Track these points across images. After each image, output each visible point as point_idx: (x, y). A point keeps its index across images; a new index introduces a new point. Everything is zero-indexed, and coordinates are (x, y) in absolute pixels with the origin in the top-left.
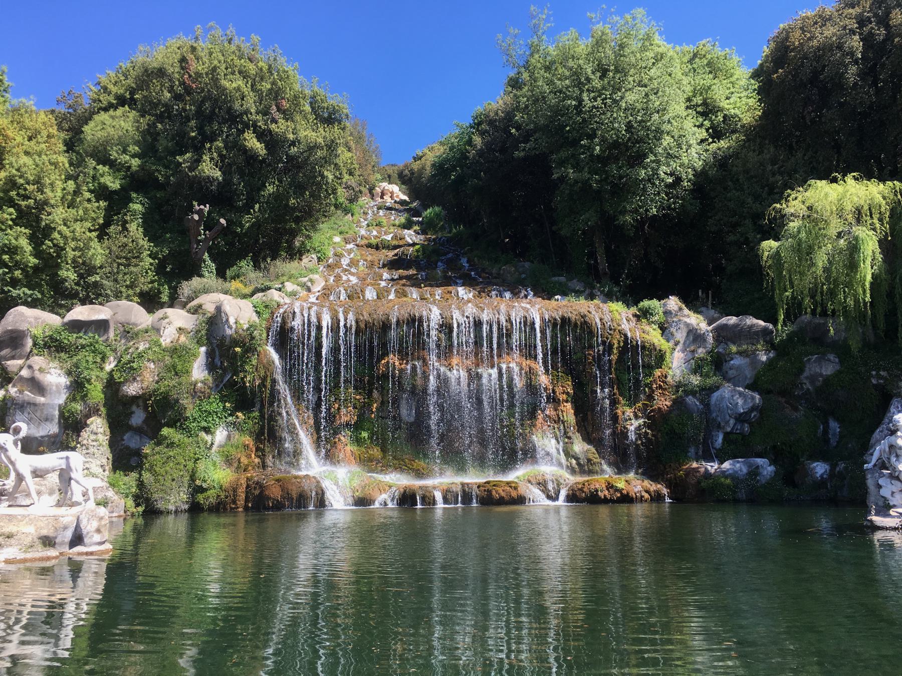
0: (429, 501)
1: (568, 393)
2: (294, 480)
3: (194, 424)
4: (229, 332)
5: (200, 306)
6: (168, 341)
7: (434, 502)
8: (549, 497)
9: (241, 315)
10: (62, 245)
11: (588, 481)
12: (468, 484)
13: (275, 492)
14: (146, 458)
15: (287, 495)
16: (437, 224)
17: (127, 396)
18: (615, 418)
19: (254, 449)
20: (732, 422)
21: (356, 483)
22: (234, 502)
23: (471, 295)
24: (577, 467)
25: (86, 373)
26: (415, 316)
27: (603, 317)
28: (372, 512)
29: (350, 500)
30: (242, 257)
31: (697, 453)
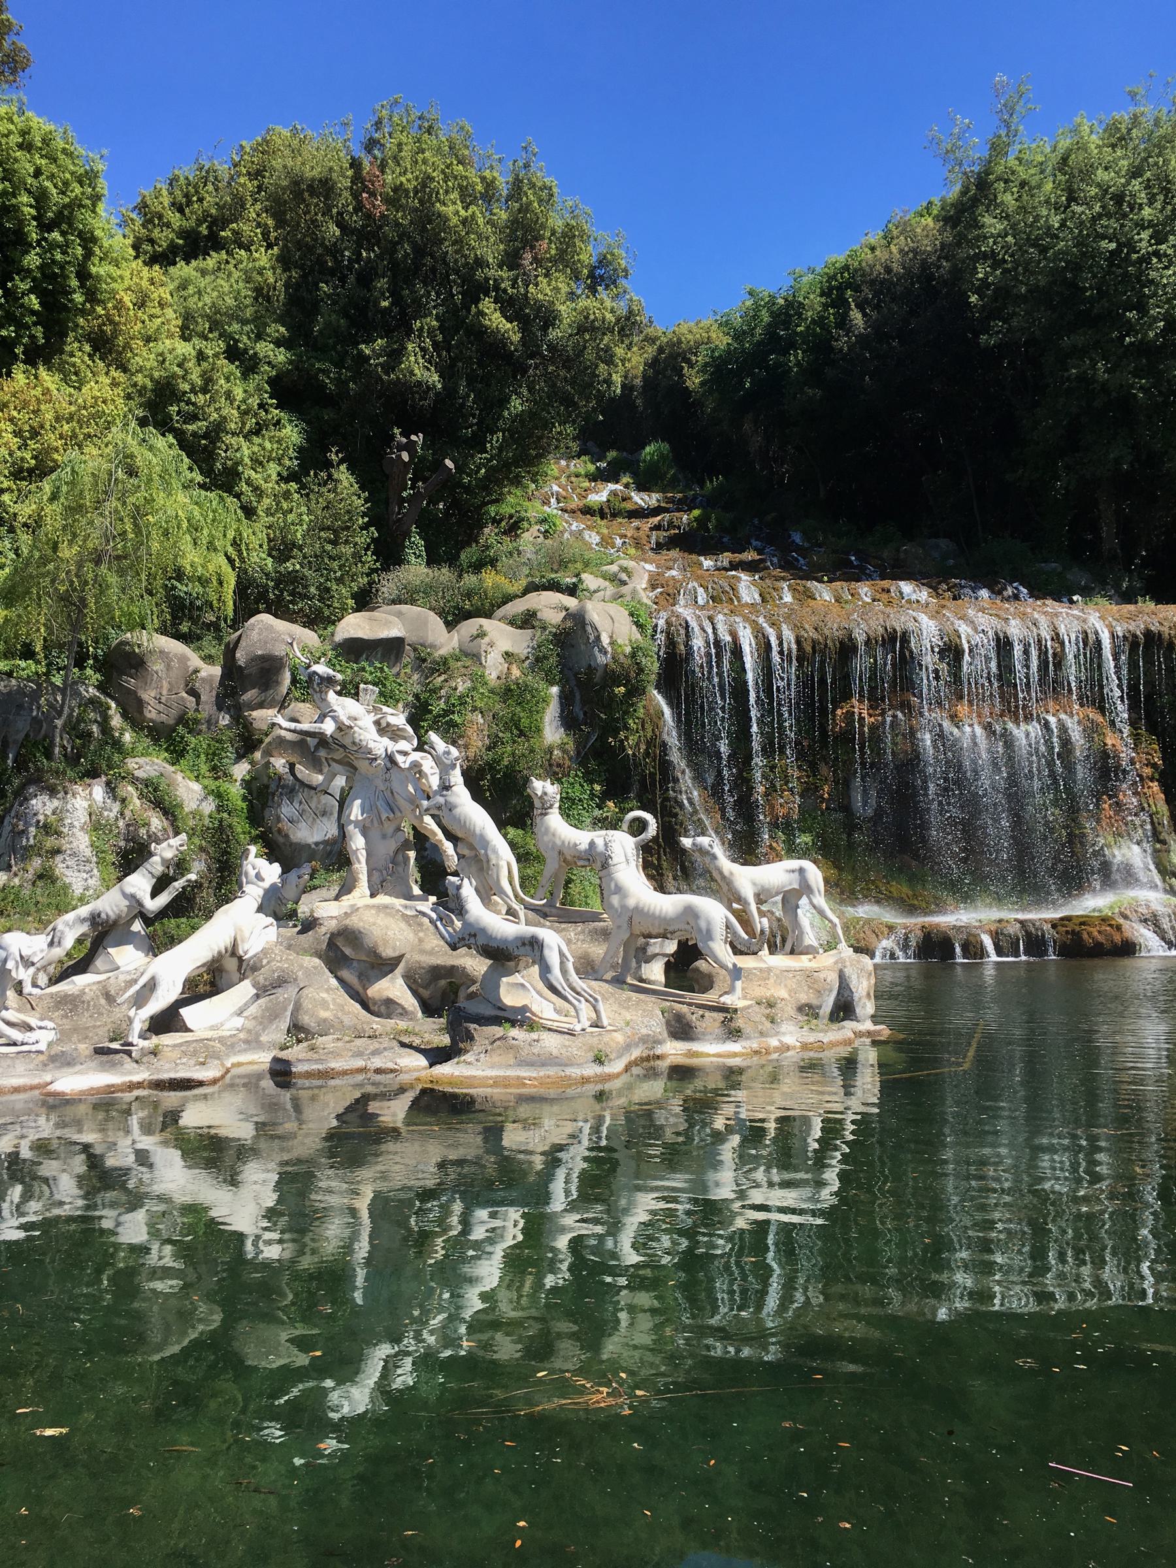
0: (973, 949)
1: (1154, 766)
4: (602, 659)
7: (982, 953)
9: (616, 630)
12: (1032, 922)
16: (666, 473)
26: (895, 630)
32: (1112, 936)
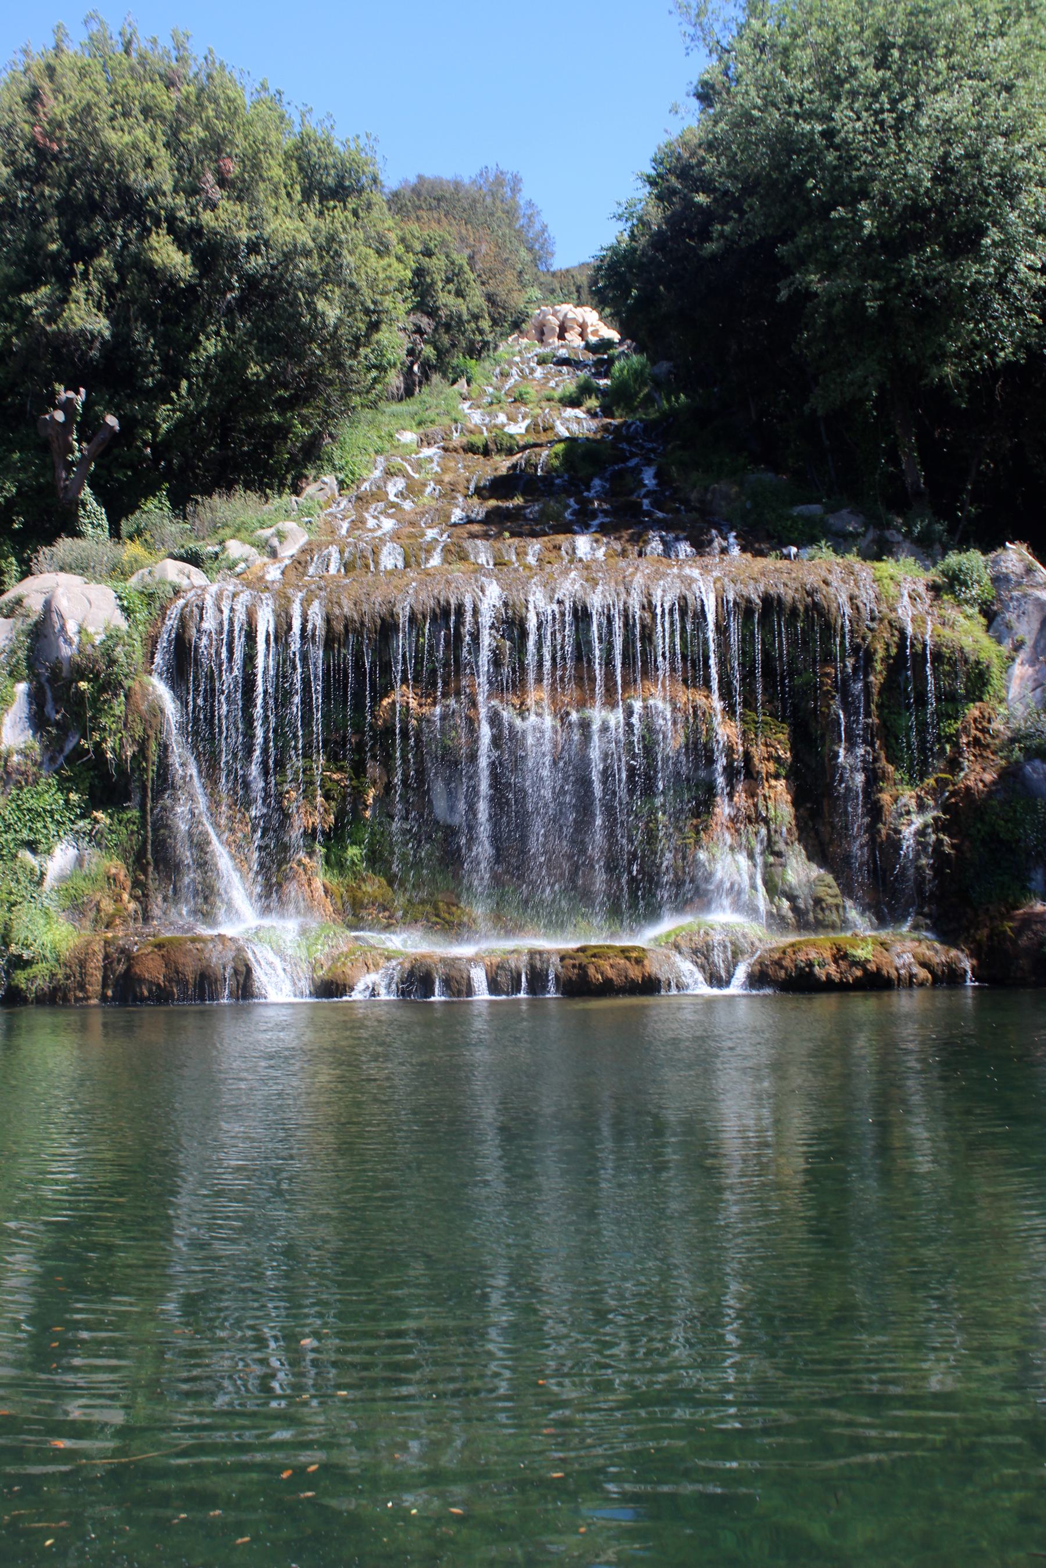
1: (778, 760)
2: (189, 945)
3: (9, 837)
4: (66, 651)
5: (19, 602)
8: (715, 980)
11: (792, 945)
12: (540, 953)
13: (153, 970)
15: (176, 975)
16: (637, 393)
18: (875, 811)
19: (128, 884)
21: (321, 952)
22: (82, 987)
23: (600, 553)
24: (790, 914)
26: (448, 603)
29: (305, 985)
30: (150, 491)
32: (626, 970)
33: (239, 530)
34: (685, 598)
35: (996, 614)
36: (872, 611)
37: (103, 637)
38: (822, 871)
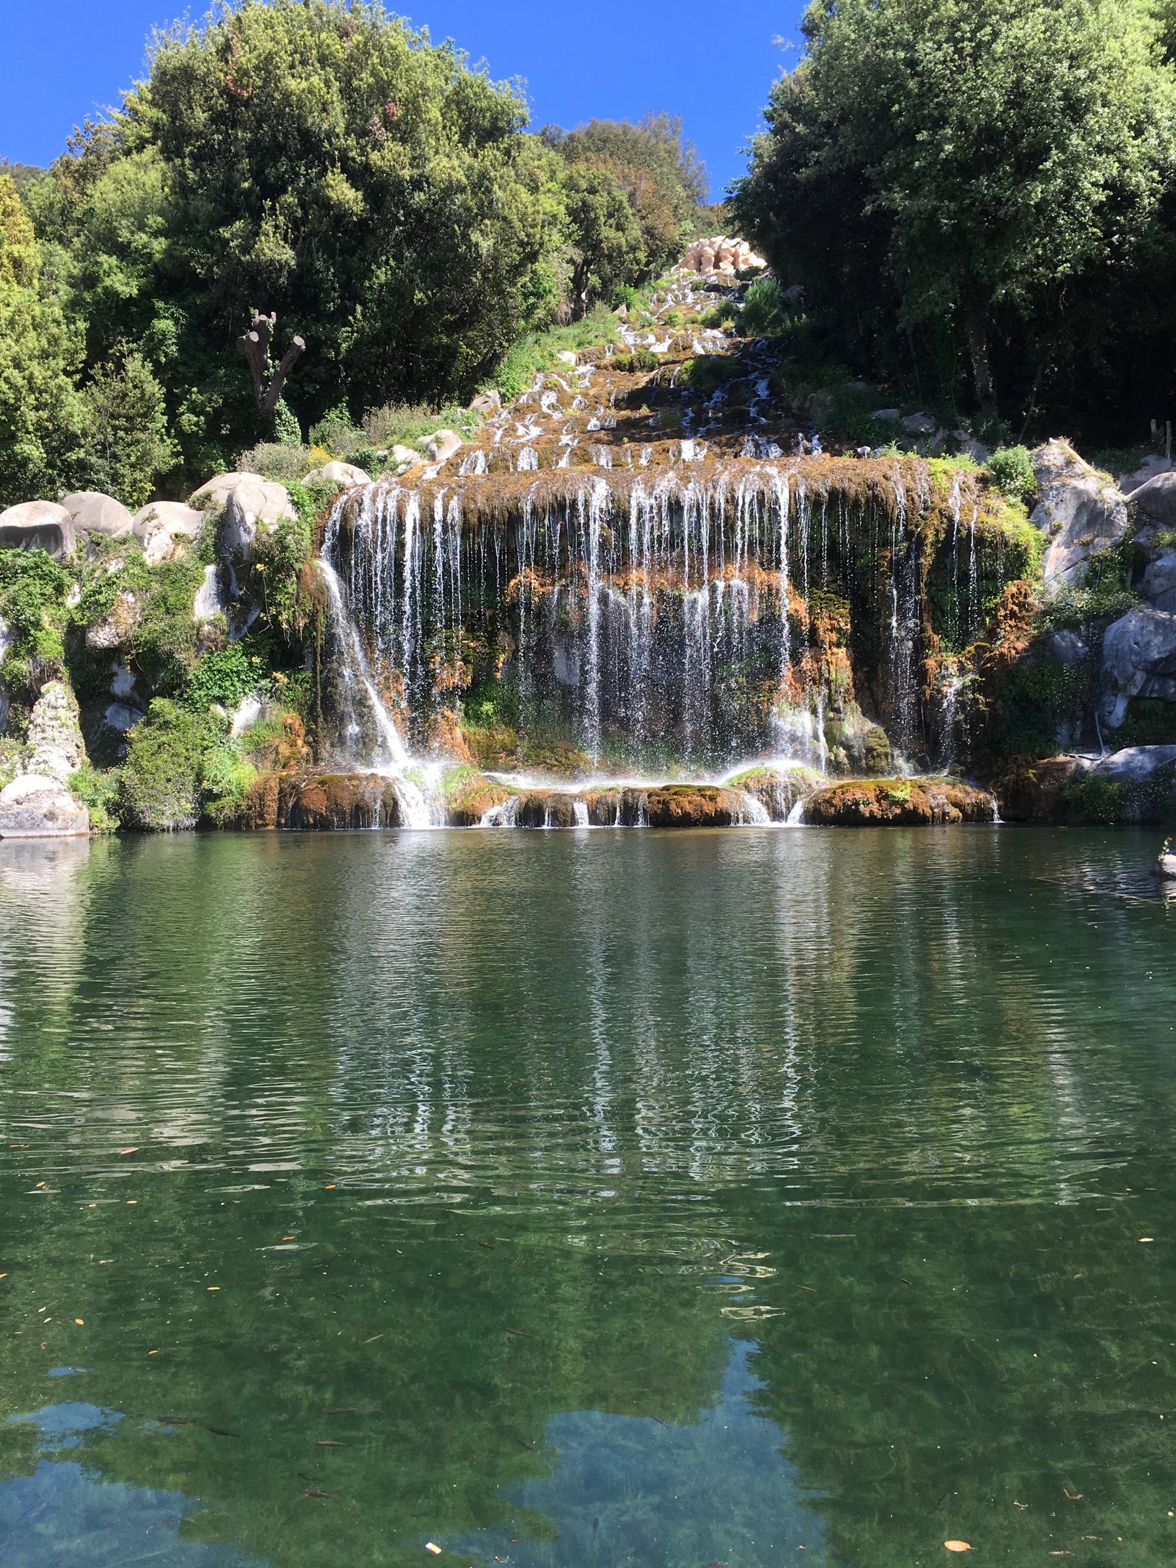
0: (563, 818)
1: (839, 630)
3: (202, 693)
4: (246, 539)
5: (208, 496)
6: (158, 556)
8: (776, 815)
10: (12, 401)
11: (842, 787)
12: (633, 791)
13: (317, 802)
14: (130, 744)
16: (767, 314)
17: (95, 648)
18: (921, 674)
19: (303, 732)
20: (1140, 677)
21: (456, 787)
22: (261, 816)
24: (846, 761)
25: (28, 612)
27: (912, 485)
28: (479, 834)
31: (1071, 736)
33: (405, 436)
34: (763, 493)
35: (1037, 502)
36: (925, 502)
37: (277, 527)
38: (874, 725)
